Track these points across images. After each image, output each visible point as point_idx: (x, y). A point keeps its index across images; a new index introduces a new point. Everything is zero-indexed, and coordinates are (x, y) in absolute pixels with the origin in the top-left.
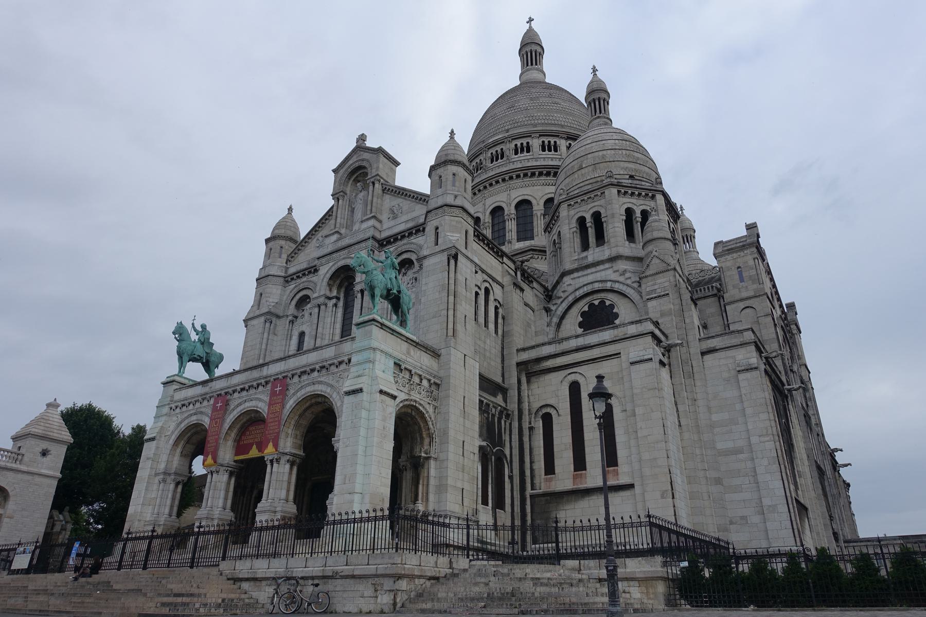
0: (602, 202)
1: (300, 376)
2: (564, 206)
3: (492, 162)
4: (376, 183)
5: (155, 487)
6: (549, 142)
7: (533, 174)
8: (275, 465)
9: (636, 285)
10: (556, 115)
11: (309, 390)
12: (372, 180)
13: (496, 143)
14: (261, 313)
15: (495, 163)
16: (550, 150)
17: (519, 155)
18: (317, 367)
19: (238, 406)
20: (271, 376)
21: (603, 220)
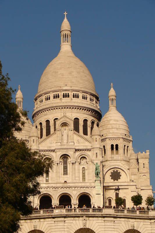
0: (119, 142)
2: (108, 139)
3: (64, 97)
6: (85, 95)
7: (81, 109)
9: (127, 169)
10: (86, 82)
11: (83, 191)
13: (66, 90)
15: (65, 98)
16: (85, 99)
17: (75, 98)
19: (61, 192)
20: (72, 186)
21: (119, 147)
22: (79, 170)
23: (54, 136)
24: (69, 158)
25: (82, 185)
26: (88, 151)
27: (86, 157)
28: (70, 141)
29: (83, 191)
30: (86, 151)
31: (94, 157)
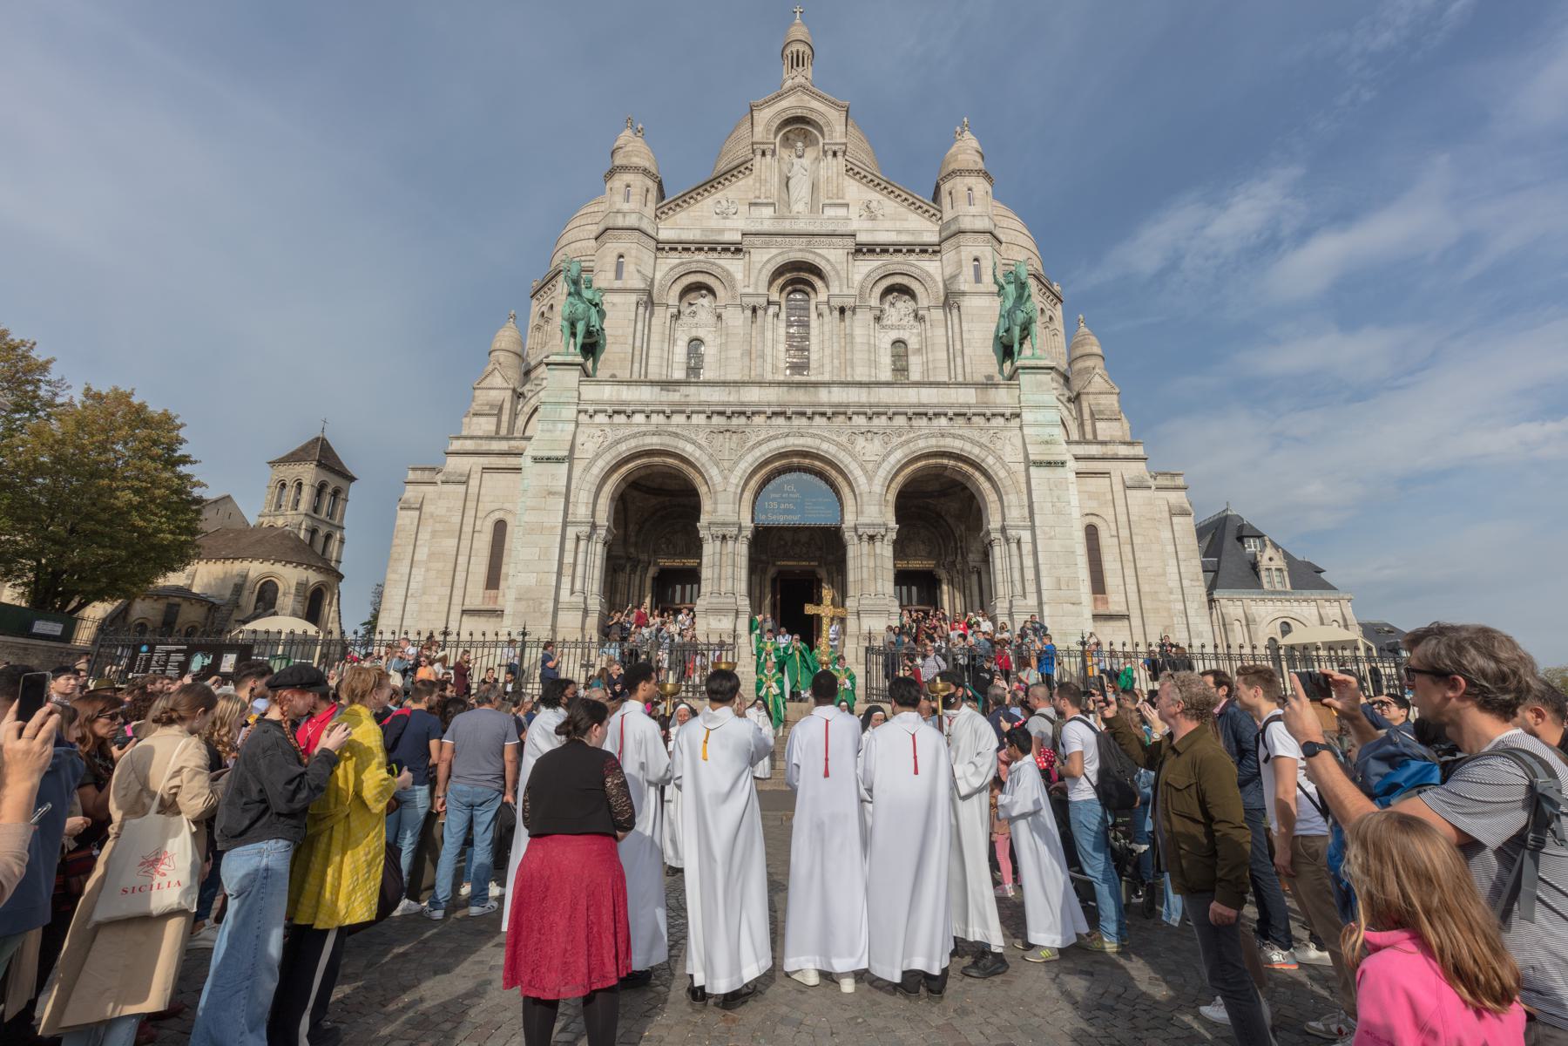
1: (910, 419)
4: (838, 154)
5: (570, 545)
8: (878, 544)
11: (932, 444)
12: (834, 148)
14: (628, 286)
18: (950, 412)
19: (769, 439)
20: (848, 406)
22: (873, 349)
23: (740, 183)
24: (819, 284)
25: (925, 400)
26: (926, 256)
27: (914, 285)
28: (827, 201)
29: (926, 437)
30: (912, 258)
31: (961, 278)
